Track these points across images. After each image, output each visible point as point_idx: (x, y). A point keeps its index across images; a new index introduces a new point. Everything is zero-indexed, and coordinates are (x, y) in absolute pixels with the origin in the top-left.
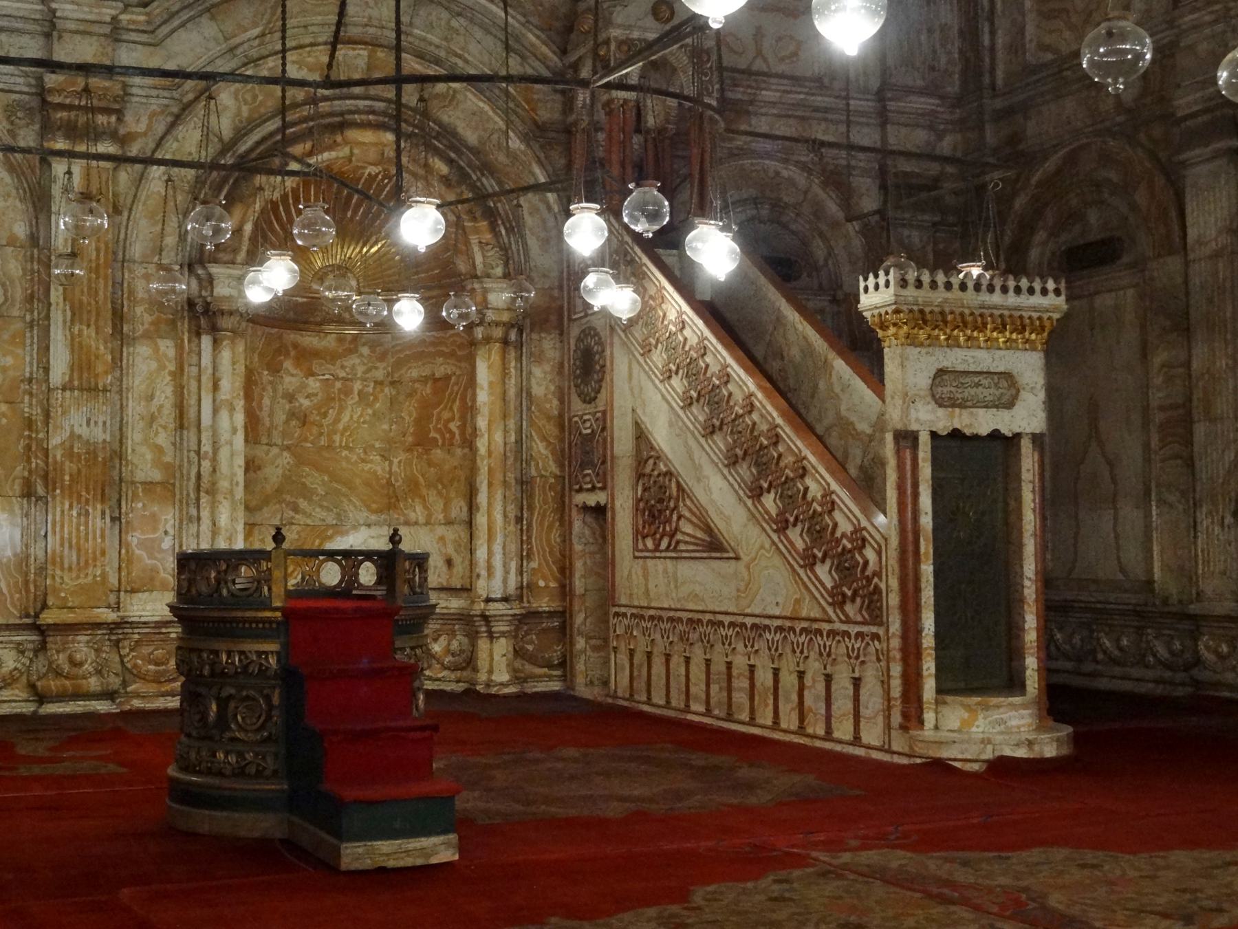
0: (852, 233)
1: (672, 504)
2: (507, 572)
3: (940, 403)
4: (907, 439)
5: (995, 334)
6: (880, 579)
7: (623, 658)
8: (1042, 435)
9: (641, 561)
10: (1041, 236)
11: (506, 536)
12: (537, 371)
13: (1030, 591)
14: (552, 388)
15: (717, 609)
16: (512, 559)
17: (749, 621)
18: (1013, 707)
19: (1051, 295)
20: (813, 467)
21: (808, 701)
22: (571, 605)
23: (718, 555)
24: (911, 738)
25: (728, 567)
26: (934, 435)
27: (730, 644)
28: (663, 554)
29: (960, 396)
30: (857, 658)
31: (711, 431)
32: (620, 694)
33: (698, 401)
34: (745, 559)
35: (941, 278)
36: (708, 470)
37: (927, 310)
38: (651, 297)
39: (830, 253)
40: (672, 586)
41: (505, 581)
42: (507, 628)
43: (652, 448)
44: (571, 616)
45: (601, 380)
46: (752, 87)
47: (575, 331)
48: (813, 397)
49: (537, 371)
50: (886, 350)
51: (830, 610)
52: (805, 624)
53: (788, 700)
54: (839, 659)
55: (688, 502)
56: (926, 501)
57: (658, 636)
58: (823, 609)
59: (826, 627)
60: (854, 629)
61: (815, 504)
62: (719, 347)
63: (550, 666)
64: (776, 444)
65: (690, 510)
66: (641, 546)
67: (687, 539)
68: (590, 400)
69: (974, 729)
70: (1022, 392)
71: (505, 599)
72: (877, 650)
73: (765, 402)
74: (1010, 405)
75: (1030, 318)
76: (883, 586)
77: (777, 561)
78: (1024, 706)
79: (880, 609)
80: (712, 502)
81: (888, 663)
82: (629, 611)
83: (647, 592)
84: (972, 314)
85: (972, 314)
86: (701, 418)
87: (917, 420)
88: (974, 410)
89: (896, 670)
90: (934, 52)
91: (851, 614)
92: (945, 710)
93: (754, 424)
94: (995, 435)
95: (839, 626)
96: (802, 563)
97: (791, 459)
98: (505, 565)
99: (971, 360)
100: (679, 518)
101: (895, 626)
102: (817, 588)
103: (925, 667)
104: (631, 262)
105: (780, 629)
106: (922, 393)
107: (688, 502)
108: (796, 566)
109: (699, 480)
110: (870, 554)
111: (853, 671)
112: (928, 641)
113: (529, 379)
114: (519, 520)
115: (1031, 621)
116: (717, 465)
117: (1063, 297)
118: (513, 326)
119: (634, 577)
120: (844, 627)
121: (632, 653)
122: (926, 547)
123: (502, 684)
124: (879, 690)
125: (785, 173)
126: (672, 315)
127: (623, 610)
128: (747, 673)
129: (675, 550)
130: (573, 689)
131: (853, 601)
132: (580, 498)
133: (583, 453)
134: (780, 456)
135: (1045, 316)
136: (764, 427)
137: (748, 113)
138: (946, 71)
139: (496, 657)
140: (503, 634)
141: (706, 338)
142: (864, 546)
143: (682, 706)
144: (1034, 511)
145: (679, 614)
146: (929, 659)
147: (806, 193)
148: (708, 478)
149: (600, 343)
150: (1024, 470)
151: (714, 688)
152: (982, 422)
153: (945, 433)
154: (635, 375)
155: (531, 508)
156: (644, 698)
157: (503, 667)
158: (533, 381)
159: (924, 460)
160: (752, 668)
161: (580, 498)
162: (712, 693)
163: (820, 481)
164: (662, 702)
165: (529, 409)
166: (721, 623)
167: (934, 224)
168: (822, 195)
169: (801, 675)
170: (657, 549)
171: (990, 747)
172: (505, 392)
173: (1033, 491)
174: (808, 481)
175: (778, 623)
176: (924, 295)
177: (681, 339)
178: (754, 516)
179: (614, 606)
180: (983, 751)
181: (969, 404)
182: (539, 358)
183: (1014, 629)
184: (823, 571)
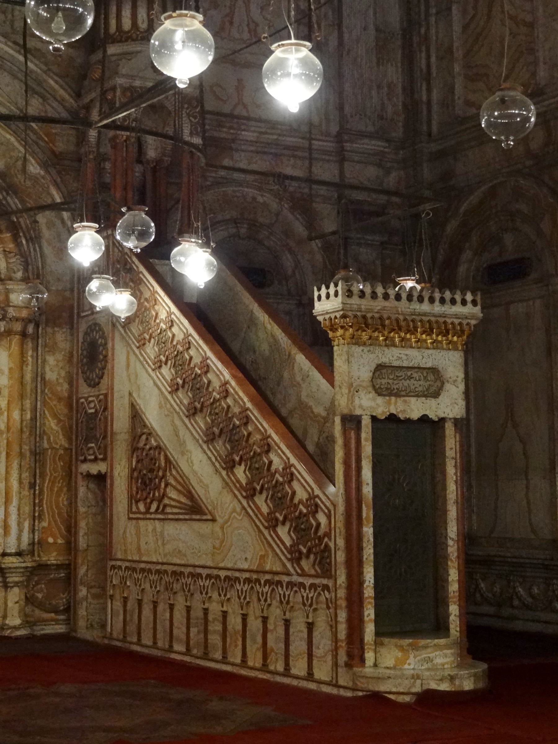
0: (316, 249)
1: (160, 474)
2: (20, 531)
3: (379, 392)
4: (352, 422)
5: (424, 336)
6: (330, 539)
7: (118, 604)
8: (462, 419)
9: (134, 522)
10: (467, 255)
11: (20, 499)
12: (51, 360)
13: (453, 549)
14: (63, 374)
15: (197, 564)
16: (25, 520)
17: (223, 574)
18: (438, 647)
19: (469, 305)
20: (276, 444)
21: (271, 643)
22: (75, 558)
23: (198, 517)
24: (354, 674)
25: (205, 528)
26: (374, 419)
27: (207, 593)
28: (153, 516)
29: (395, 387)
30: (311, 605)
31: (193, 412)
32: (115, 635)
33: (183, 387)
34: (220, 520)
35: (380, 290)
36: (191, 445)
37: (369, 315)
38: (146, 300)
39: (297, 264)
40: (160, 543)
41: (19, 538)
42: (21, 579)
43: (145, 426)
44: (75, 569)
45: (104, 368)
46: (234, 129)
47: (83, 327)
48: (279, 384)
49: (51, 360)
50: (335, 348)
51: (289, 565)
52: (268, 577)
53: (254, 641)
54: (297, 607)
55: (174, 472)
56: (367, 474)
57: (147, 586)
58: (284, 565)
59: (286, 579)
60: (308, 582)
61: (277, 475)
62: (201, 342)
63: (57, 612)
64: (246, 424)
65: (176, 479)
66: (134, 509)
67: (173, 503)
68: (94, 384)
69: (406, 666)
70: (446, 384)
71: (19, 554)
72: (327, 599)
73: (237, 388)
74: (436, 395)
75: (452, 323)
76: (332, 545)
77: (246, 522)
78: (447, 647)
79: (330, 564)
80: (195, 473)
81: (336, 609)
82: (124, 565)
83: (139, 549)
84: (405, 319)
85: (405, 319)
86: (186, 402)
87: (361, 406)
89: (342, 616)
90: (383, 104)
91: (306, 568)
92: (383, 651)
93: (229, 407)
94: (424, 419)
95: (295, 579)
96: (266, 524)
97: (258, 437)
98: (20, 524)
99: (404, 357)
100: (167, 485)
101: (342, 579)
102: (278, 546)
103: (366, 614)
104: (130, 270)
105: (248, 581)
106: (364, 384)
107: (174, 472)
108: (261, 527)
109: (183, 454)
110: (322, 518)
111: (308, 617)
112: (369, 591)
113: (43, 367)
114: (32, 486)
115: (453, 575)
116: (197, 441)
117: (479, 308)
118: (30, 321)
119: (128, 535)
120: (301, 580)
121: (125, 600)
122: (367, 513)
123: (15, 628)
124: (329, 633)
125: (260, 199)
126: (163, 315)
127: (119, 563)
128: (221, 619)
129: (163, 512)
130: (76, 631)
131: (308, 557)
132: (84, 468)
133: (88, 428)
134: (249, 434)
135: (465, 322)
136: (237, 410)
137: (231, 149)
138: (392, 120)
139: (10, 604)
140: (16, 584)
141: (190, 335)
142: (317, 512)
143: (167, 646)
144: (456, 482)
145: (165, 567)
146: (369, 606)
147: (277, 215)
148: (191, 453)
149: (103, 337)
150: (447, 449)
151: (194, 631)
152: (414, 408)
153: (383, 418)
154: (132, 364)
155: (43, 476)
156: (135, 639)
157: (16, 613)
158: (47, 369)
159: (366, 440)
160: (225, 614)
161: (84, 468)
162: (192, 635)
163: (282, 455)
164: (150, 643)
165: (43, 392)
166: (200, 575)
167: (382, 243)
168: (290, 217)
169: (265, 620)
170: (148, 511)
171: (419, 682)
172: (22, 377)
173: (455, 466)
174: (272, 456)
175: (247, 575)
176: (366, 303)
177: (170, 335)
178: (227, 484)
179: (111, 560)
180: (413, 685)
181: (403, 393)
182: (52, 349)
183: (440, 581)
184: (283, 531)
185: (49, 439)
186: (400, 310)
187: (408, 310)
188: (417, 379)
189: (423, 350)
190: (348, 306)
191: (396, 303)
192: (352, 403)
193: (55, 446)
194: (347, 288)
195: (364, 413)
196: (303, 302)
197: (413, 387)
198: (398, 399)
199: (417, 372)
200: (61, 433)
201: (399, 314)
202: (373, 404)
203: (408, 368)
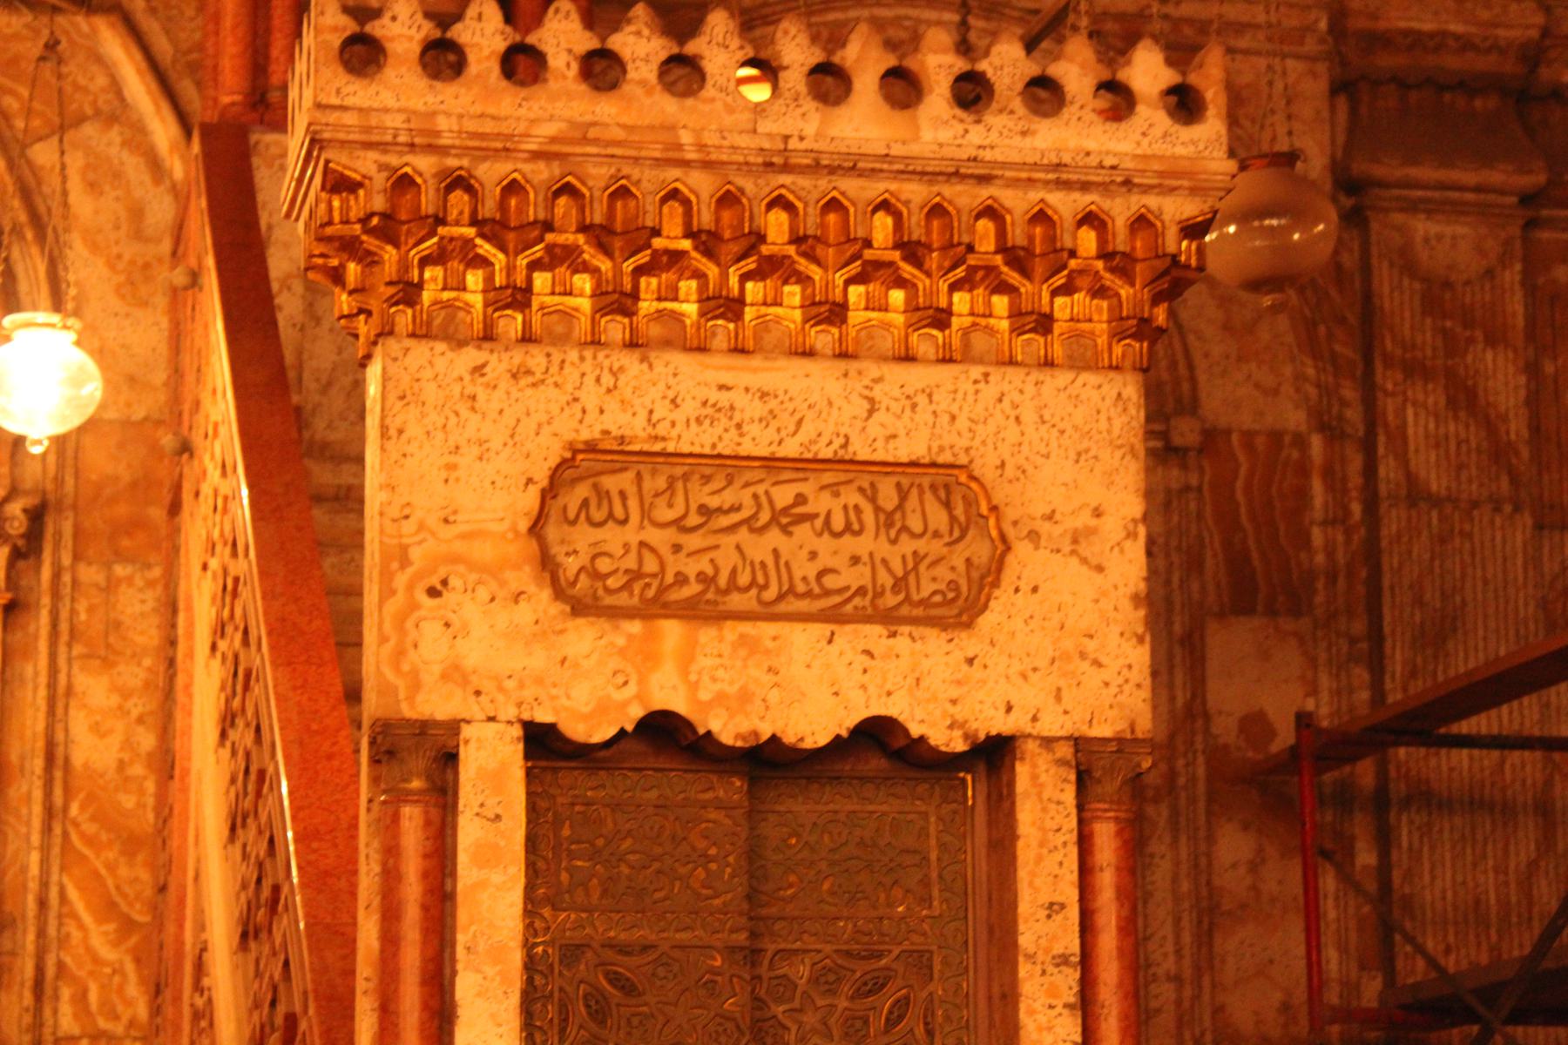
8: (1122, 744)
12: (94, 689)
19: (1151, 118)
26: (543, 743)
29: (692, 568)
37: (490, 174)
70: (1022, 549)
74: (959, 609)
75: (1041, 217)
85: (728, 199)
87: (455, 673)
88: (767, 629)
106: (484, 551)
135: (1120, 210)
152: (805, 686)
158: (78, 723)
167: (1528, 199)
181: (736, 601)
185: (81, 998)
186: (686, 138)
187: (743, 141)
188: (838, 523)
189: (873, 369)
190: (350, 119)
191: (669, 106)
192: (400, 653)
193: (102, 1023)
194: (350, 26)
195: (474, 709)
196: (1177, 441)
197: (804, 569)
198: (707, 634)
199: (834, 489)
200: (132, 977)
201: (685, 164)
202: (537, 660)
203: (771, 463)
